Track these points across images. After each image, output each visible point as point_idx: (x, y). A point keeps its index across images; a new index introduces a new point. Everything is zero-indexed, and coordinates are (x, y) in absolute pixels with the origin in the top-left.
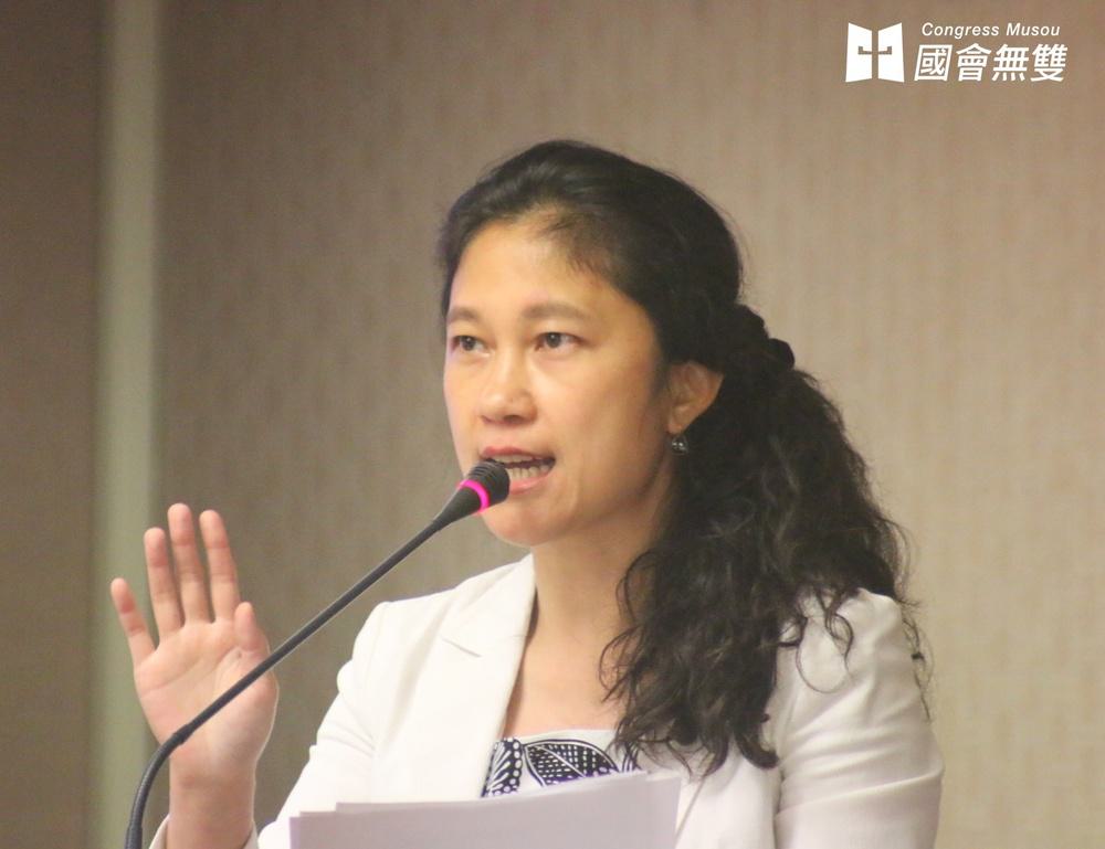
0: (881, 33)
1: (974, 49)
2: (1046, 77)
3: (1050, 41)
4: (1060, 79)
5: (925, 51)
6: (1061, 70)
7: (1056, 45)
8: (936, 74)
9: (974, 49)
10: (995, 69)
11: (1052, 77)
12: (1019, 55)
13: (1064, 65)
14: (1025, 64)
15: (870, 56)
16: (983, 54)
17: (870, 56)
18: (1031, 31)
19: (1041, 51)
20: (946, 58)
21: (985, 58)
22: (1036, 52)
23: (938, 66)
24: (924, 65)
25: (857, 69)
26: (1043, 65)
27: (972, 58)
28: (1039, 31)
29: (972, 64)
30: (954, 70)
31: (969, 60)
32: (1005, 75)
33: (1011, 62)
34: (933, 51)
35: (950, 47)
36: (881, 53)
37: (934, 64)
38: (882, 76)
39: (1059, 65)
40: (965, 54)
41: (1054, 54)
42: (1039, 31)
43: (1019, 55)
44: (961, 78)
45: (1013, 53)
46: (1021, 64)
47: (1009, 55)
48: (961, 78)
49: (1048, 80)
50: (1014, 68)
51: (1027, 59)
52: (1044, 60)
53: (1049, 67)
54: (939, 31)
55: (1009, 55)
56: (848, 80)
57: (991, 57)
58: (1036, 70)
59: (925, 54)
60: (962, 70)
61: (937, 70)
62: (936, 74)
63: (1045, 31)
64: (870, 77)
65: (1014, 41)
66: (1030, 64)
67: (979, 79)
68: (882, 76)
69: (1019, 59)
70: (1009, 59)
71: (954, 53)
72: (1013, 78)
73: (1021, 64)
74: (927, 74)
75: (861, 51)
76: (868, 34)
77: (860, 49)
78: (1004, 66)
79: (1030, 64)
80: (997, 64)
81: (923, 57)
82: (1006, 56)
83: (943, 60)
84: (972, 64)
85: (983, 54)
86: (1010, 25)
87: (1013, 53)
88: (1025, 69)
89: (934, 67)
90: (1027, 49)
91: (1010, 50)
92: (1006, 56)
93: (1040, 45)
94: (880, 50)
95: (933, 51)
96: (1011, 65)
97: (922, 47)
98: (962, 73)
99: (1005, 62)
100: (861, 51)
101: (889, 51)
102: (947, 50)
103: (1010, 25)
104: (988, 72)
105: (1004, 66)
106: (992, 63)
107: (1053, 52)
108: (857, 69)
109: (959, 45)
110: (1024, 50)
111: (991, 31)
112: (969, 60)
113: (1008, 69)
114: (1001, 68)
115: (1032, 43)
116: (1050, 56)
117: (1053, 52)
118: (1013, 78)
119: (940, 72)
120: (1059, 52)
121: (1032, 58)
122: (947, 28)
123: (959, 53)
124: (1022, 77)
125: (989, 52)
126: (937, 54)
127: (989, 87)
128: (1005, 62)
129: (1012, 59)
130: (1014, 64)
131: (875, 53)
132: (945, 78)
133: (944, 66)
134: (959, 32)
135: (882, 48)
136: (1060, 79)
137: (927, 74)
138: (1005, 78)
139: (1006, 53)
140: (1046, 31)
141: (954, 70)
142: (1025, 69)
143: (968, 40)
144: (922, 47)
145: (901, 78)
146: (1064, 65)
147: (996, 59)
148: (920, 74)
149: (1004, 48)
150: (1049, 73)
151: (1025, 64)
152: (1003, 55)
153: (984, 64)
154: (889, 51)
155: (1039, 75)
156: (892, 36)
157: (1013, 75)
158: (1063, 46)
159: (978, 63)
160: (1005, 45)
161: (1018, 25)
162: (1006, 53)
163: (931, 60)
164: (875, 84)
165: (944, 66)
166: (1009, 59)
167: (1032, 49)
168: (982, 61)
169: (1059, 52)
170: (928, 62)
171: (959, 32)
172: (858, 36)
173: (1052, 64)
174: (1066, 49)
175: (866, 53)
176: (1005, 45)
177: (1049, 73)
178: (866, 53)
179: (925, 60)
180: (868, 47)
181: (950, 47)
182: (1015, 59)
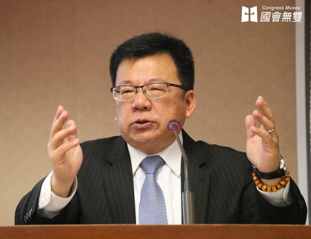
0: (251, 9)
1: (277, 13)
2: (296, 21)
3: (298, 11)
4: (300, 21)
5: (263, 13)
6: (301, 19)
7: (299, 12)
8: (266, 20)
9: (277, 13)
10: (282, 19)
11: (298, 21)
12: (289, 15)
14: (291, 17)
15: (248, 15)
16: (279, 14)
17: (248, 15)
18: (292, 8)
20: (269, 15)
21: (280, 16)
22: (294, 14)
23: (267, 18)
24: (263, 17)
27: (276, 16)
29: (276, 17)
30: (271, 19)
31: (275, 16)
32: (285, 20)
33: (287, 17)
34: (266, 13)
35: (270, 13)
37: (266, 18)
38: (251, 21)
39: (300, 17)
41: (299, 15)
43: (289, 15)
44: (273, 21)
45: (287, 14)
46: (290, 17)
48: (273, 21)
50: (288, 18)
51: (291, 16)
52: (296, 16)
54: (267, 8)
56: (242, 22)
57: (281, 15)
58: (294, 19)
60: (273, 19)
61: (267, 19)
62: (266, 20)
64: (248, 21)
65: (288, 11)
66: (292, 17)
67: (278, 21)
68: (251, 21)
70: (286, 16)
72: (288, 21)
73: (290, 17)
74: (264, 20)
75: (246, 14)
76: (248, 9)
78: (285, 18)
79: (292, 17)
80: (283, 17)
81: (263, 15)
82: (285, 15)
84: (276, 17)
85: (279, 14)
86: (287, 7)
87: (287, 14)
88: (291, 19)
89: (266, 18)
90: (291, 13)
91: (287, 13)
92: (285, 15)
93: (295, 12)
94: (251, 13)
95: (266, 13)
96: (287, 18)
97: (262, 13)
99: (285, 17)
100: (246, 14)
101: (253, 14)
102: (269, 13)
103: (287, 7)
104: (281, 19)
105: (285, 18)
106: (282, 17)
108: (245, 19)
109: (273, 12)
111: (281, 8)
112: (275, 16)
113: (286, 18)
114: (284, 18)
117: (298, 14)
118: (288, 21)
119: (267, 19)
121: (293, 16)
123: (272, 14)
124: (290, 21)
125: (281, 14)
126: (266, 15)
127: (281, 24)
128: (285, 17)
130: (288, 17)
131: (249, 14)
132: (269, 21)
133: (268, 18)
135: (251, 13)
136: (300, 21)
137: (264, 20)
138: (285, 21)
139: (286, 14)
141: (271, 19)
142: (291, 19)
144: (262, 13)
145: (257, 22)
147: (283, 16)
149: (285, 13)
150: (297, 20)
151: (291, 17)
153: (280, 17)
155: (294, 20)
156: (254, 9)
159: (278, 17)
160: (285, 12)
161: (289, 6)
162: (286, 14)
163: (265, 16)
164: (250, 23)
165: (268, 18)
166: (286, 16)
167: (293, 13)
168: (279, 16)
170: (264, 17)
171: (273, 8)
172: (245, 9)
173: (298, 17)
176: (285, 12)
177: (297, 20)
179: (263, 16)
180: (248, 13)
181: (270, 13)
182: (288, 16)
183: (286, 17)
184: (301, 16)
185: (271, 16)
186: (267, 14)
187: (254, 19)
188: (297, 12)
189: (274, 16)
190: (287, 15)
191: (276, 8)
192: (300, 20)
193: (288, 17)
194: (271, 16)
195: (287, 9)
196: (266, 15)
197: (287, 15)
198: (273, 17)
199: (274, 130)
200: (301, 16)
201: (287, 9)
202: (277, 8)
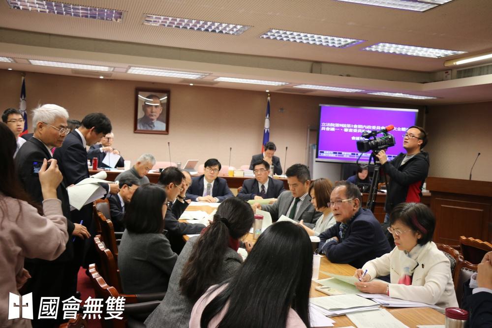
1: (72, 300)
2: (113, 317)
4: (121, 318)
5: (44, 300)
6: (122, 312)
7: (119, 297)
8: (50, 315)
9: (72, 300)
10: (84, 312)
11: (116, 317)
12: (98, 304)
13: (123, 310)
15: (19, 307)
16: (77, 303)
20: (56, 305)
21: (78, 305)
22: (108, 302)
23: (51, 310)
24: (44, 309)
26: (111, 309)
27: (71, 305)
29: (71, 309)
30: (61, 313)
31: (69, 307)
32: (90, 315)
34: (49, 300)
35: (58, 298)
36: (24, 306)
37: (50, 308)
39: (120, 309)
40: (67, 303)
41: (118, 303)
43: (98, 304)
44: (65, 318)
45: (94, 302)
47: (92, 303)
48: (65, 318)
49: (114, 318)
50: (95, 311)
51: (102, 306)
52: (112, 306)
53: (115, 311)
55: (92, 303)
57: (82, 304)
58: (108, 312)
59: (44, 303)
60: (65, 312)
61: (51, 312)
66: (104, 309)
67: (75, 318)
69: (98, 306)
70: (92, 306)
71: (61, 300)
72: (94, 318)
74: (45, 315)
75: (15, 305)
77: (15, 304)
78: (89, 310)
79: (104, 309)
80: (85, 309)
81: (43, 304)
82: (90, 304)
84: (71, 307)
85: (77, 303)
87: (94, 302)
88: (101, 312)
89: (49, 311)
90: (102, 300)
91: (93, 300)
92: (90, 304)
93: (110, 297)
95: (49, 300)
97: (42, 298)
98: (65, 314)
99: (90, 308)
100: (15, 305)
105: (89, 310)
106: (82, 309)
107: (117, 301)
110: (101, 300)
112: (69, 307)
113: (91, 312)
114: (87, 311)
116: (116, 304)
117: (117, 301)
118: (94, 318)
119: (53, 314)
121: (105, 305)
123: (63, 302)
125: (80, 301)
126: (51, 303)
128: (90, 308)
129: (94, 306)
130: (95, 309)
131: (21, 306)
132: (55, 318)
133: (55, 310)
135: (24, 303)
136: (121, 318)
137: (45, 315)
138: (90, 318)
139: (91, 302)
141: (61, 313)
142: (101, 312)
144: (42, 298)
146: (123, 310)
147: (85, 306)
149: (89, 299)
150: (113, 314)
152: (88, 303)
155: (109, 316)
157: (94, 316)
159: (74, 309)
160: (90, 297)
162: (91, 302)
163: (48, 306)
165: (55, 310)
166: (92, 306)
167: (106, 299)
168: (77, 307)
170: (46, 308)
172: (14, 298)
173: (117, 309)
174: (125, 300)
175: (18, 306)
176: (90, 297)
177: (115, 315)
178: (18, 306)
179: (44, 306)
180: (18, 303)
181: (58, 298)
182: (96, 306)
184: (124, 303)
185: (61, 305)
186: (51, 301)
187: (28, 314)
188: (114, 297)
189: (66, 307)
190: (94, 304)
192: (119, 316)
193: (95, 309)
194: (61, 305)
197: (94, 304)
198: (64, 309)
200: (124, 303)
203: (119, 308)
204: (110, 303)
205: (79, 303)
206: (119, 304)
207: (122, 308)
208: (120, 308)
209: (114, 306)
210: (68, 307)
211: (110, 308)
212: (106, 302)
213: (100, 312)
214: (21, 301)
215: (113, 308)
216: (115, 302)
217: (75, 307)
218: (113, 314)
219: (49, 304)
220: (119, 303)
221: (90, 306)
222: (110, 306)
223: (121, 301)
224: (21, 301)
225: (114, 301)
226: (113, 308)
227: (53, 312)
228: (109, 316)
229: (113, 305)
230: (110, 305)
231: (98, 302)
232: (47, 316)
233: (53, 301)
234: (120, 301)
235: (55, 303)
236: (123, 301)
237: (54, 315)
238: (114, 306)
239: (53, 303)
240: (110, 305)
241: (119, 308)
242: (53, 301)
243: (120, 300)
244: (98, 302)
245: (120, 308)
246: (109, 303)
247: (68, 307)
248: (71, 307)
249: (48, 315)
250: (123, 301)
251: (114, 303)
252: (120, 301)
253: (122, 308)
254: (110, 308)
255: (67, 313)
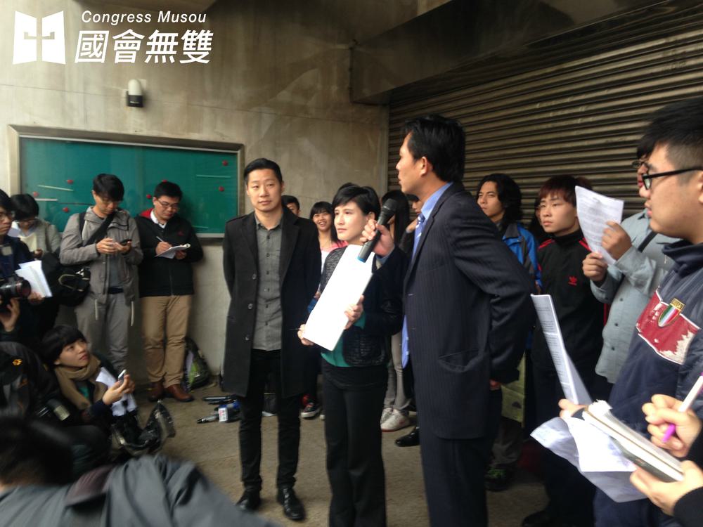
0: (43, 19)
1: (129, 35)
2: (194, 59)
3: (198, 27)
4: (206, 62)
5: (84, 36)
6: (207, 53)
7: (203, 31)
8: (94, 57)
9: (129, 35)
10: (148, 52)
13: (210, 49)
16: (137, 39)
17: (35, 41)
18: (180, 18)
19: (188, 36)
20: (103, 42)
21: (139, 42)
22: (185, 37)
23: (96, 50)
24: (84, 49)
25: (24, 52)
26: (191, 48)
27: (127, 43)
28: (188, 18)
29: (127, 47)
30: (111, 54)
31: (124, 45)
32: (156, 57)
33: (162, 47)
34: (92, 36)
35: (107, 33)
36: (47, 38)
39: (205, 48)
40: (120, 39)
42: (188, 18)
44: (117, 61)
45: (164, 38)
46: (171, 48)
47: (161, 39)
48: (117, 61)
49: (196, 62)
50: (165, 52)
51: (177, 44)
52: (192, 44)
53: (196, 51)
55: (161, 39)
57: (144, 42)
58: (185, 53)
59: (84, 39)
60: (118, 53)
61: (95, 53)
62: (94, 57)
63: (193, 18)
64: (35, 59)
65: (166, 28)
66: (179, 48)
67: (133, 61)
68: (43, 60)
69: (169, 43)
70: (160, 43)
72: (164, 60)
73: (171, 48)
74: (87, 57)
75: (26, 36)
76: (35, 19)
78: (156, 49)
79: (179, 48)
80: (149, 48)
81: (82, 42)
82: (157, 40)
83: (101, 44)
85: (137, 39)
86: (161, 13)
87: (164, 38)
88: (175, 52)
90: (177, 35)
91: (161, 35)
92: (157, 40)
93: (188, 31)
94: (43, 35)
95: (92, 36)
96: (162, 49)
99: (156, 47)
100: (26, 36)
101: (52, 36)
102: (104, 35)
103: (161, 13)
105: (156, 49)
106: (145, 47)
111: (144, 18)
112: (124, 45)
113: (159, 52)
114: (153, 52)
115: (181, 29)
116: (198, 40)
117: (200, 37)
118: (164, 60)
119: (98, 55)
120: (205, 37)
121: (181, 43)
122: (104, 15)
123: (115, 37)
125: (142, 37)
126: (95, 39)
128: (156, 47)
129: (163, 43)
130: (165, 48)
132: (102, 60)
133: (102, 49)
134: (115, 18)
135: (46, 33)
136: (206, 62)
137: (87, 57)
138: (156, 61)
139: (158, 38)
140: (193, 18)
141: (111, 54)
142: (175, 52)
143: (123, 26)
145: (61, 59)
146: (210, 49)
147: (149, 44)
148: (80, 57)
150: (193, 56)
152: (155, 40)
153: (138, 48)
154: (52, 36)
157: (164, 57)
158: (209, 31)
159: (132, 47)
160: (157, 31)
161: (169, 13)
162: (158, 38)
163: (90, 44)
165: (102, 49)
166: (160, 43)
167: (182, 34)
168: (136, 45)
169: (205, 37)
170: (87, 46)
172: (25, 23)
173: (199, 48)
174: (212, 34)
175: (32, 38)
176: (157, 31)
178: (32, 38)
179: (84, 44)
180: (33, 33)
181: (107, 33)
182: (166, 43)
183: (159, 48)
184: (211, 39)
185: (112, 42)
186: (96, 36)
188: (194, 31)
189: (119, 45)
190: (163, 40)
191: (125, 18)
193: (165, 48)
194: (112, 42)
195: (163, 21)
196: (95, 39)
197: (163, 40)
198: (116, 48)
199: (81, 292)
200: (211, 39)
201: (163, 21)
202: (128, 18)
203: (202, 46)
204: (189, 40)
205: (139, 39)
206: (203, 41)
207: (208, 46)
208: (205, 46)
209: (195, 44)
210: (122, 45)
211: (188, 46)
212: (183, 38)
213: (172, 52)
214: (39, 30)
215: (193, 47)
216: (197, 38)
217: (133, 45)
218: (193, 56)
219: (92, 42)
220: (203, 39)
221: (157, 43)
222: (188, 44)
223: (207, 37)
224: (39, 30)
225: (195, 37)
226: (193, 47)
227: (98, 52)
228: (190, 59)
229: (194, 42)
230: (189, 42)
231: (170, 38)
232: (89, 58)
233: (98, 37)
234: (204, 37)
235: (103, 39)
236: (209, 37)
237: (101, 57)
238: (195, 44)
239: (99, 39)
240: (189, 42)
241: (202, 46)
242: (98, 37)
243: (204, 35)
244: (170, 38)
245: (205, 46)
246: (187, 39)
247: (122, 45)
248: (127, 45)
249: (90, 56)
250: (209, 37)
251: (195, 40)
252: (204, 37)
253: (208, 46)
254: (188, 47)
255: (120, 55)
